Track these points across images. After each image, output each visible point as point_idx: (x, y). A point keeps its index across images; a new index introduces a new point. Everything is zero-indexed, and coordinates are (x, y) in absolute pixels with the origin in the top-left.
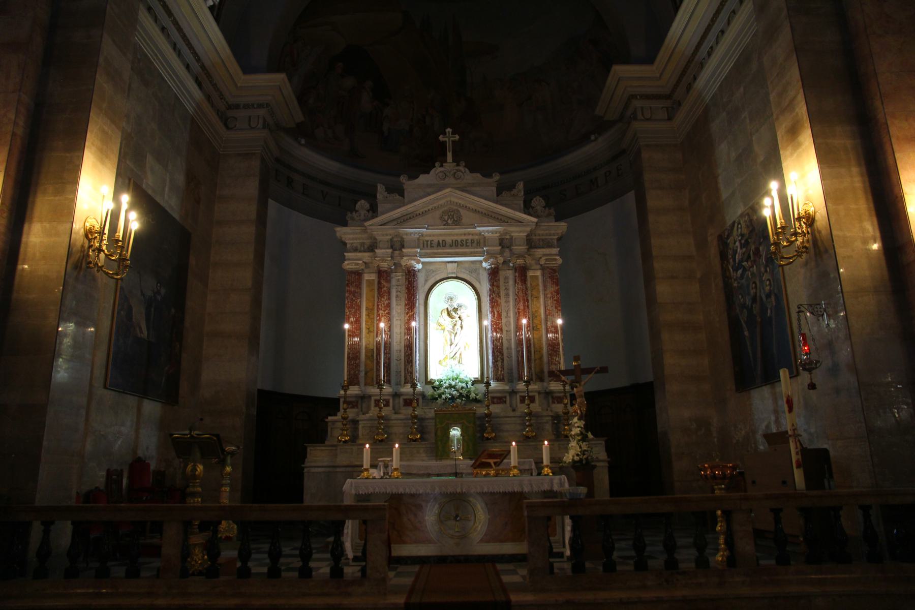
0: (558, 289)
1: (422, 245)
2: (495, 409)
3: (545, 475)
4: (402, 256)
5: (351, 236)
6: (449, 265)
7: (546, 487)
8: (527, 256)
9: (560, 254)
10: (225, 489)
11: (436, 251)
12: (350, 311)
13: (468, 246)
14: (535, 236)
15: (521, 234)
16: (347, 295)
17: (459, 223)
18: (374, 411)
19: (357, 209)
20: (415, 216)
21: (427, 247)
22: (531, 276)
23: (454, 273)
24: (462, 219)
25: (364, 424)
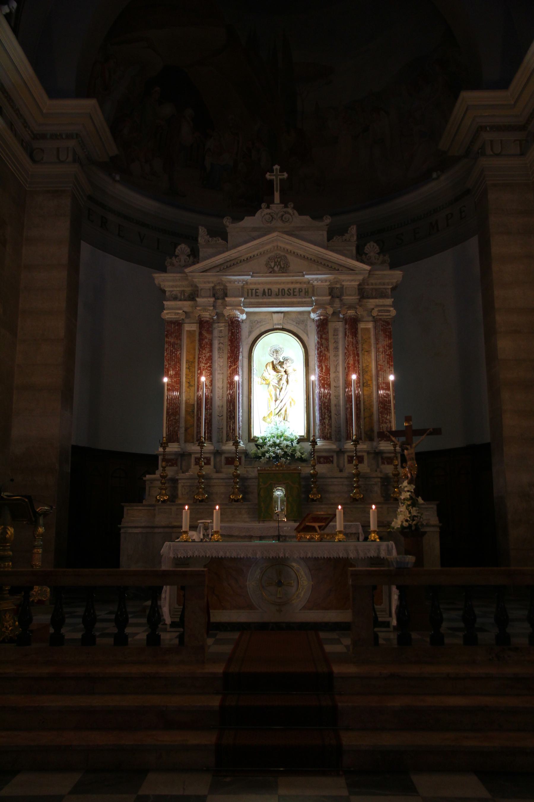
0: (391, 343)
1: (246, 294)
2: (321, 469)
3: (372, 541)
4: (225, 305)
5: (171, 283)
6: (275, 316)
7: (373, 554)
8: (358, 307)
9: (394, 305)
10: (37, 551)
11: (261, 300)
12: (169, 364)
13: (296, 295)
14: (368, 285)
15: (353, 283)
16: (166, 346)
17: (286, 270)
18: (194, 470)
19: (176, 254)
20: (239, 262)
21: (252, 295)
22: (363, 329)
23: (278, 324)
24: (289, 266)
25: (184, 483)
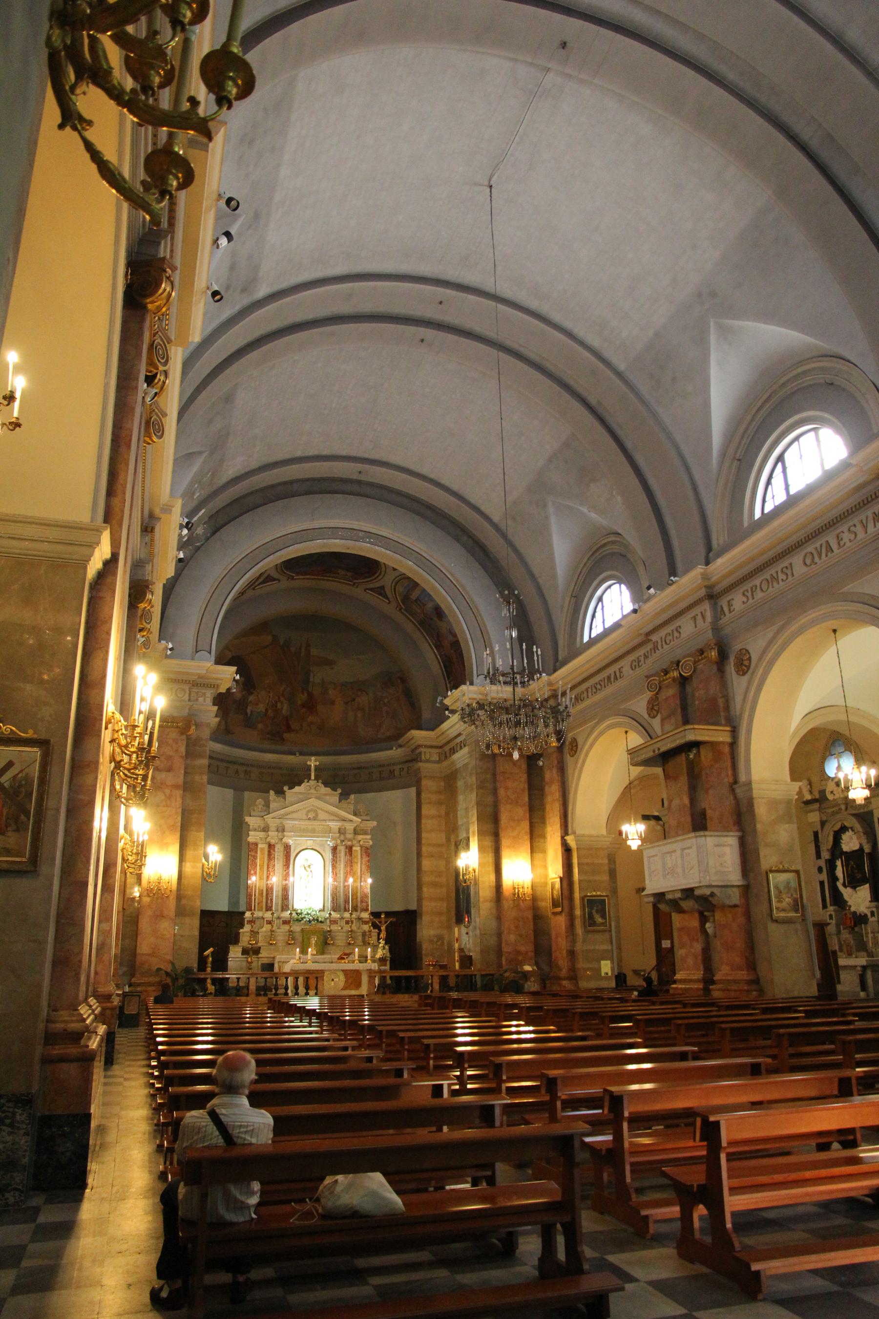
2: (334, 927)
6: (308, 841)
7: (369, 968)
9: (371, 839)
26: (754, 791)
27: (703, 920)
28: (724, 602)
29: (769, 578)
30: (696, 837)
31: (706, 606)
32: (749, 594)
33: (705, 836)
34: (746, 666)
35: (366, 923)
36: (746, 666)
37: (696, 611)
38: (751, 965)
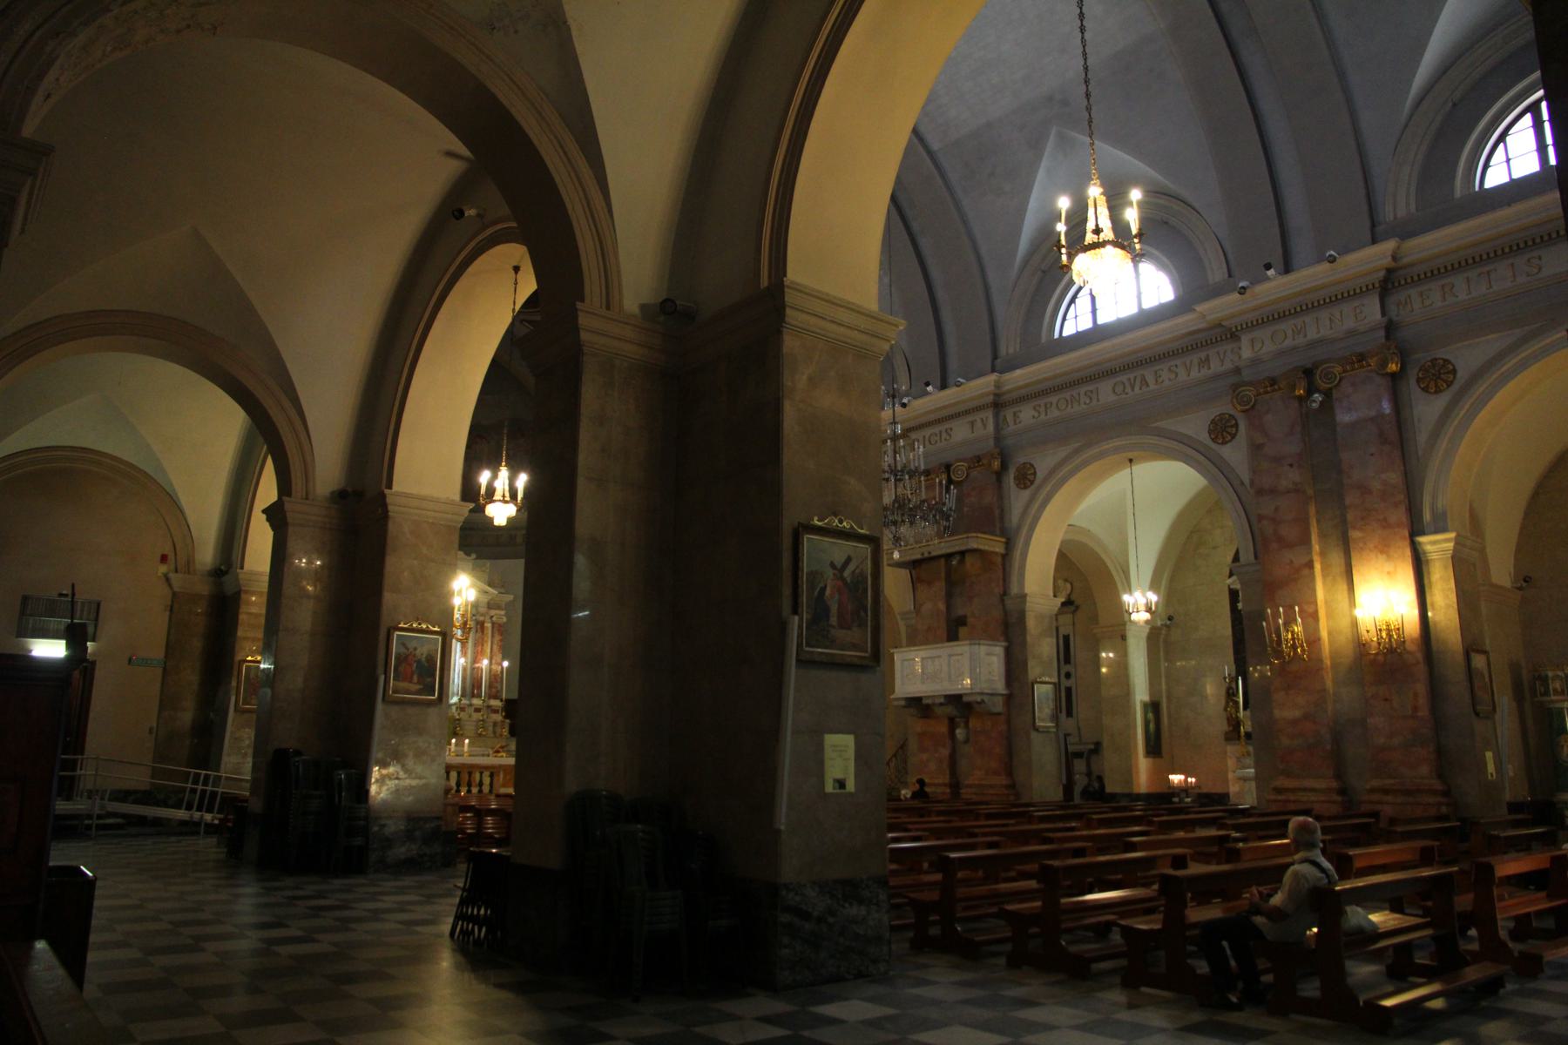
9: (505, 615)
26: (1028, 604)
27: (952, 724)
28: (1008, 414)
29: (1069, 398)
30: (971, 644)
31: (989, 415)
32: (1042, 409)
33: (979, 644)
34: (1030, 481)
35: (496, 711)
36: (1030, 481)
37: (977, 417)
38: (1009, 772)
